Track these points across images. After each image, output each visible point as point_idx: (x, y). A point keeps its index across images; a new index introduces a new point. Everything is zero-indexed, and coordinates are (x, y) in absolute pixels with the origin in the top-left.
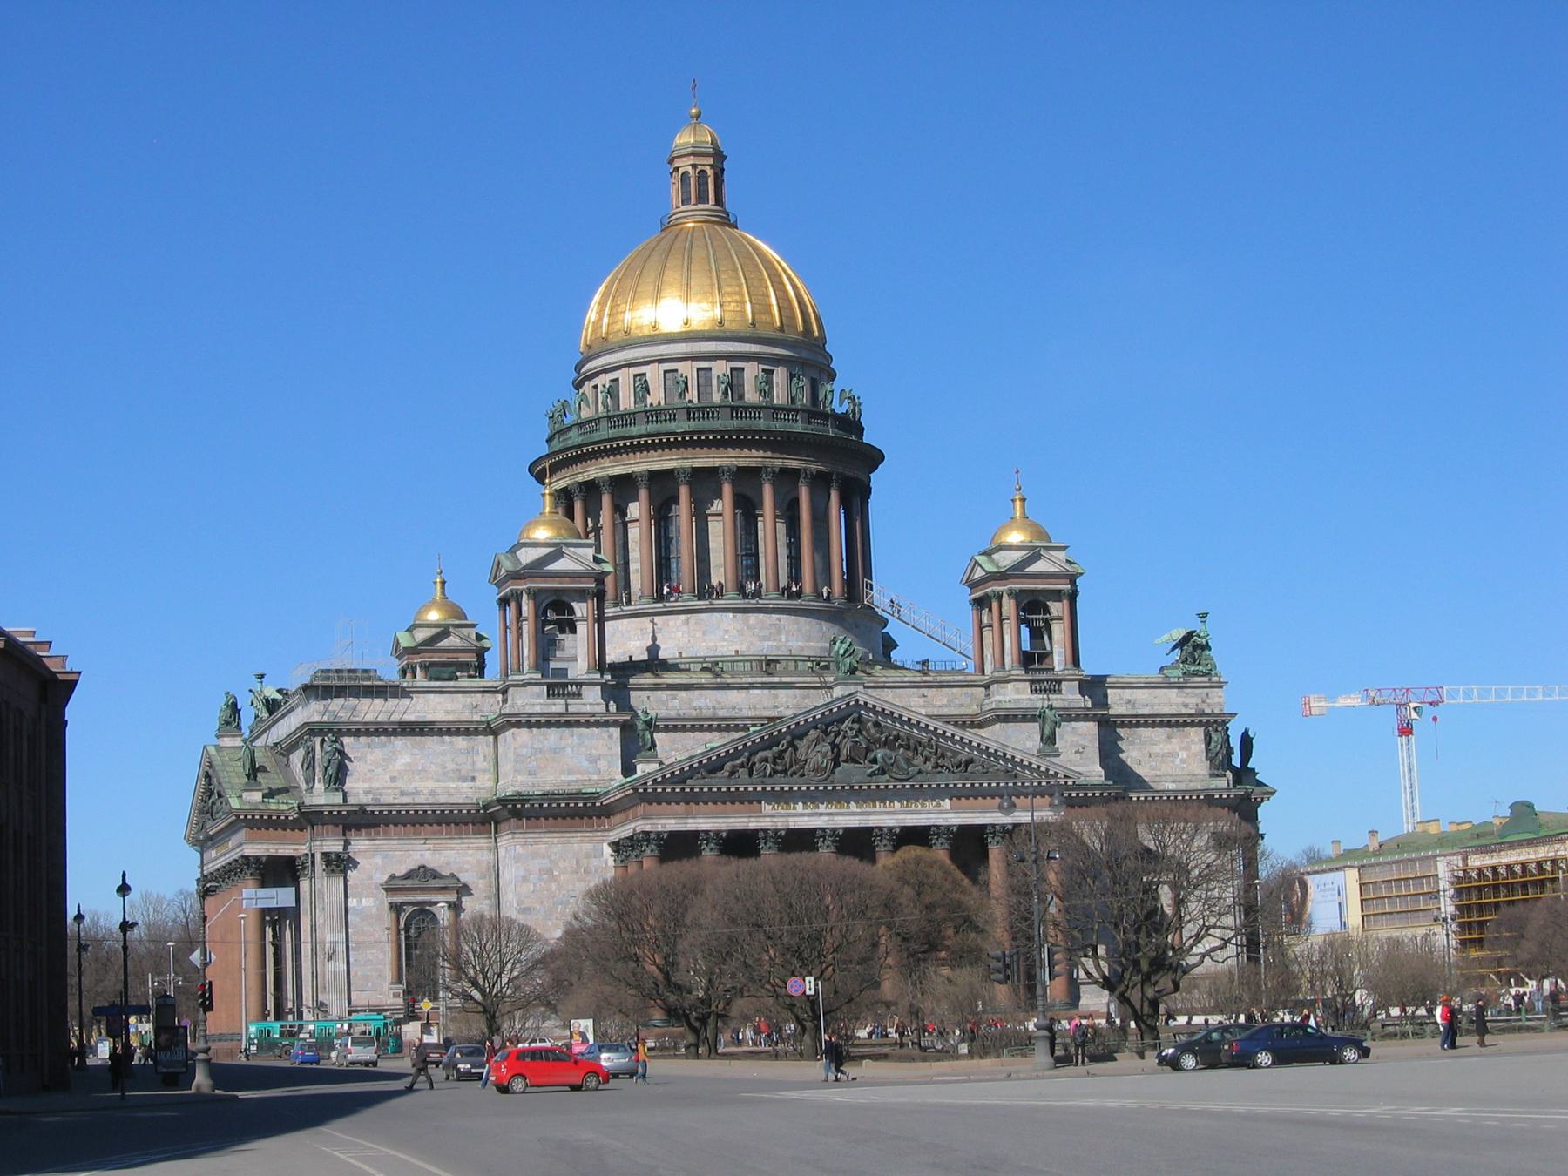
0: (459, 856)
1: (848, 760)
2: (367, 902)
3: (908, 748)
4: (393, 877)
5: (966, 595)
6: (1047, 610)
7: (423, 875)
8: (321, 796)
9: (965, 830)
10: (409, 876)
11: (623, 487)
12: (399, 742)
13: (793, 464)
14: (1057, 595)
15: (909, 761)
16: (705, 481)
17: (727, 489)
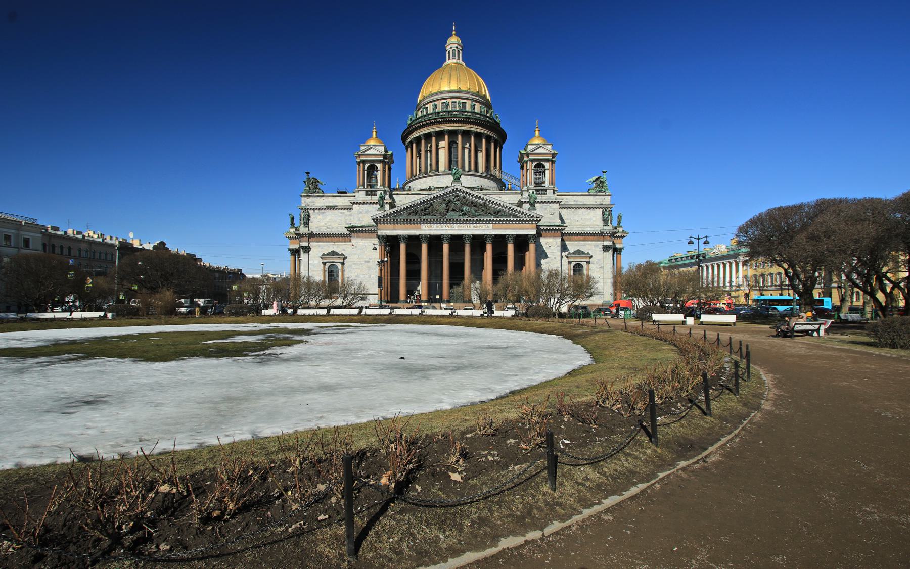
0: (340, 247)
1: (453, 210)
2: (316, 262)
3: (475, 206)
4: (324, 254)
5: (519, 165)
6: (544, 167)
7: (333, 253)
8: (303, 229)
9: (496, 236)
10: (328, 254)
11: (418, 140)
12: (329, 212)
13: (468, 129)
14: (547, 160)
15: (476, 211)
16: (440, 135)
17: (446, 137)
